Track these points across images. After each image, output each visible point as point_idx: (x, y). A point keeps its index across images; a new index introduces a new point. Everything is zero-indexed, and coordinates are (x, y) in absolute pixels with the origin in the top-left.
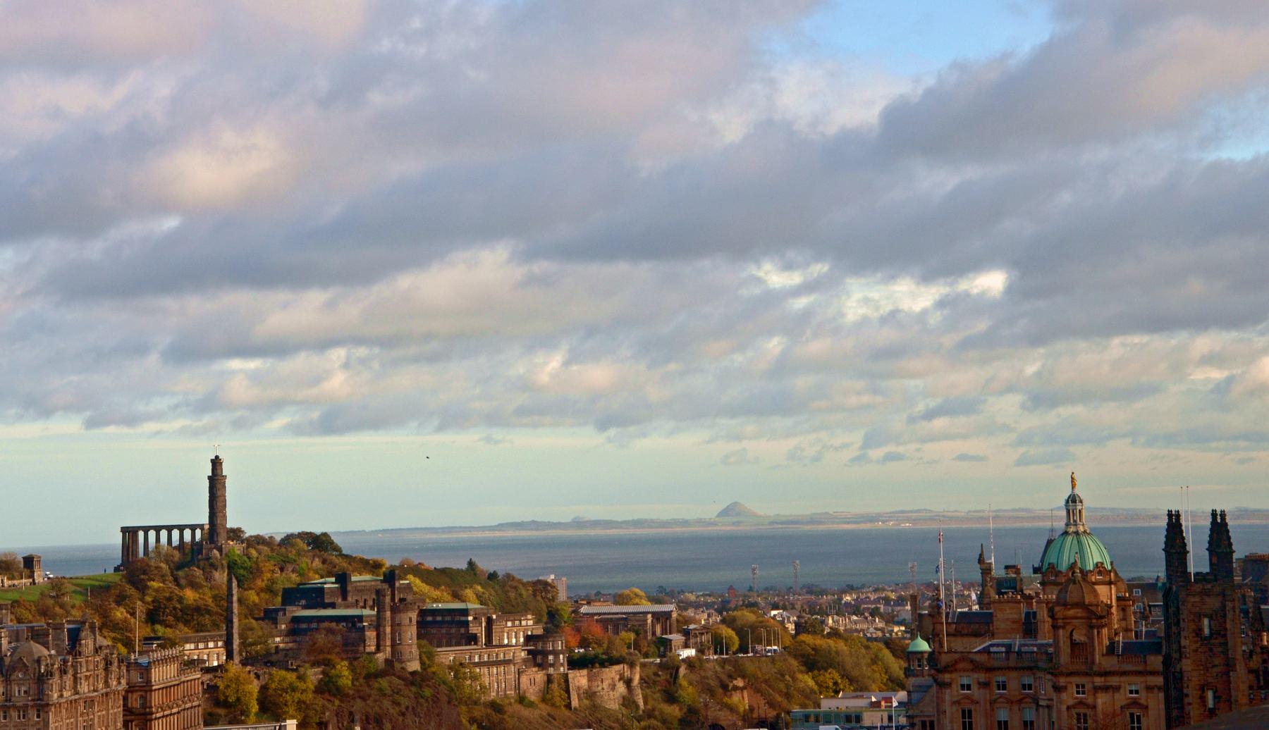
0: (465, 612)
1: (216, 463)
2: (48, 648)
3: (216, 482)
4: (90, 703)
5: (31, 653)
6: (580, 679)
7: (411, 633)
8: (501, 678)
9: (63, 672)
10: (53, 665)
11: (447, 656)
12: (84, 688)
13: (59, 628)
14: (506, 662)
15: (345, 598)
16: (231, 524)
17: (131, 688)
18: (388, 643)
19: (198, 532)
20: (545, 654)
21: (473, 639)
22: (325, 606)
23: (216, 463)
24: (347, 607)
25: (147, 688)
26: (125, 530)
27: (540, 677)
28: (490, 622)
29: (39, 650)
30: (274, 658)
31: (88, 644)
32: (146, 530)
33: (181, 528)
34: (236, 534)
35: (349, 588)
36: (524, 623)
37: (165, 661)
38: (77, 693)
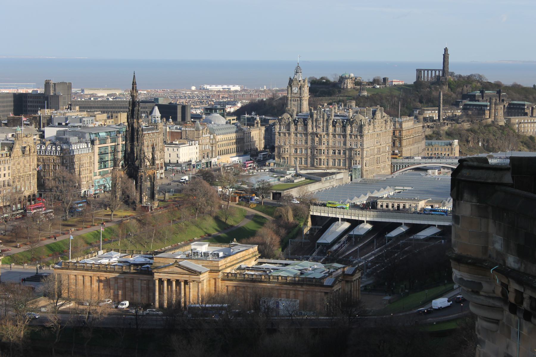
0: (524, 105)
1: (446, 50)
3: (446, 56)
7: (501, 113)
11: (515, 120)
12: (378, 130)
15: (483, 99)
18: (493, 115)
22: (476, 101)
23: (446, 50)
24: (483, 101)
26: (417, 70)
28: (533, 108)
30: (455, 118)
31: (378, 115)
32: (424, 70)
33: (435, 70)
34: (452, 74)
37: (408, 121)
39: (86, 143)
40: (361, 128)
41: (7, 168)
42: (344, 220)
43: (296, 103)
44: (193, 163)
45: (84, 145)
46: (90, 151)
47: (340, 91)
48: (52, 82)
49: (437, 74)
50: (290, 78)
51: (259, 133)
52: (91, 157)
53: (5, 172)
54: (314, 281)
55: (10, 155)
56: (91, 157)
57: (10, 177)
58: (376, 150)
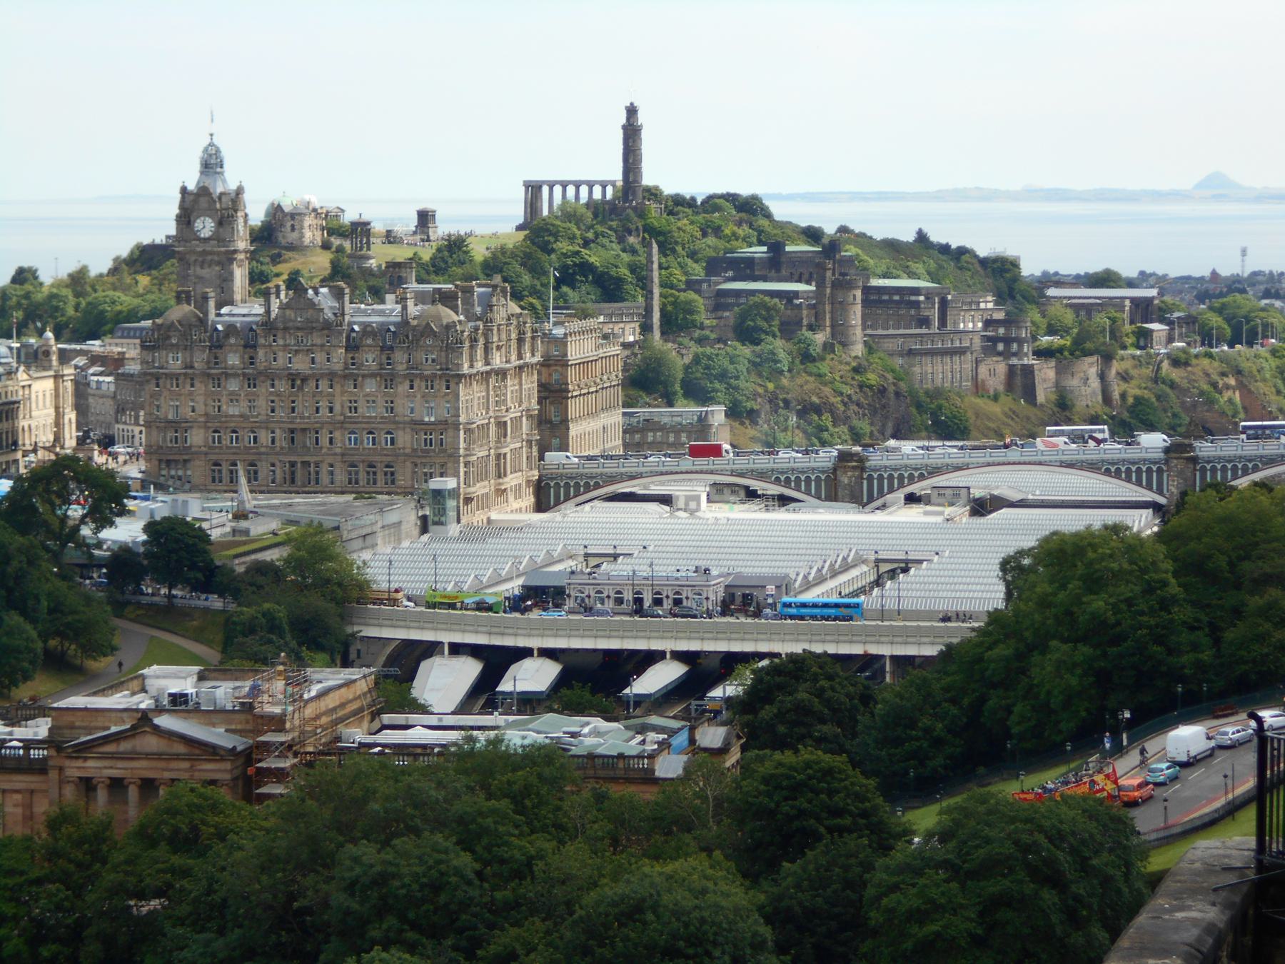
0: (916, 291)
1: (632, 111)
2: (457, 313)
3: (631, 133)
4: (502, 374)
5: (438, 318)
6: (1046, 373)
8: (957, 367)
10: (463, 332)
13: (469, 291)
14: (961, 352)
15: (778, 271)
16: (648, 179)
17: (547, 363)
19: (609, 190)
20: (1007, 341)
21: (925, 322)
22: (755, 279)
23: (632, 111)
24: (780, 280)
26: (528, 185)
27: (1001, 368)
28: (944, 303)
29: (448, 315)
32: (551, 185)
33: (591, 185)
34: (653, 193)
35: (783, 259)
36: (982, 306)
38: (487, 363)
42: (456, 649)
43: (205, 272)
47: (279, 255)
51: (56, 389)
54: (621, 765)
58: (493, 428)
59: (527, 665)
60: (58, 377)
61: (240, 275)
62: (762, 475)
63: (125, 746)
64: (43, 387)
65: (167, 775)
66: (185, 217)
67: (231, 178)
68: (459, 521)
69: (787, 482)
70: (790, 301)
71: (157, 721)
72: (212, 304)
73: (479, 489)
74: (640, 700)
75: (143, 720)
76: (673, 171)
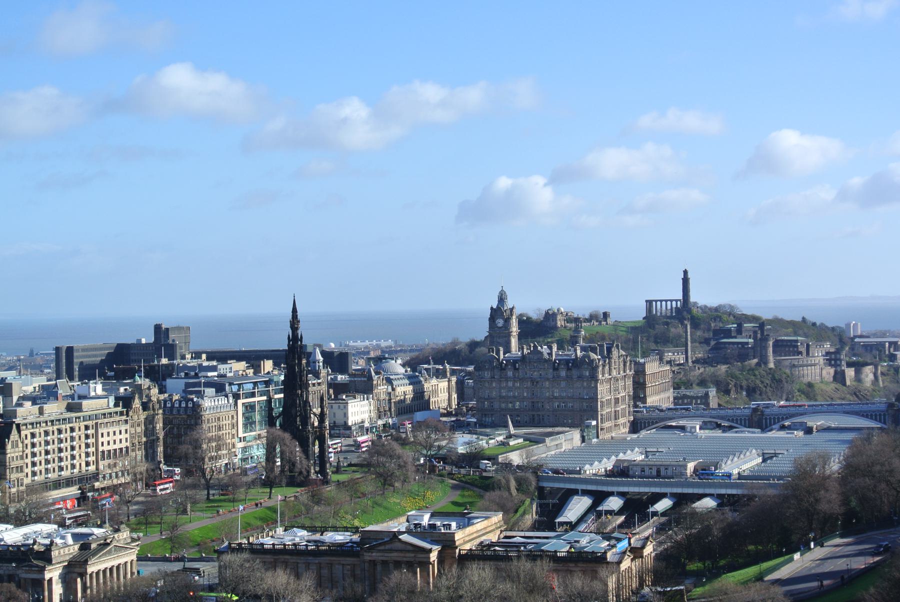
0: (797, 341)
1: (685, 272)
3: (686, 281)
9: (604, 366)
11: (788, 359)
12: (614, 373)
13: (601, 346)
14: (815, 365)
20: (836, 360)
21: (800, 353)
22: (732, 337)
23: (685, 272)
25: (643, 372)
26: (647, 301)
28: (808, 346)
29: (593, 356)
31: (615, 353)
32: (656, 301)
33: (671, 301)
39: (227, 396)
40: (594, 369)
41: (123, 432)
44: (367, 425)
45: (223, 401)
46: (232, 408)
48: (164, 326)
49: (674, 306)
50: (492, 308)
52: (233, 417)
53: (121, 437)
55: (127, 415)
56: (233, 417)
57: (128, 444)
58: (613, 401)
59: (611, 498)
60: (449, 381)
61: (514, 342)
62: (722, 418)
63: (388, 547)
64: (443, 384)
65: (405, 559)
66: (492, 319)
67: (509, 304)
68: (598, 437)
69: (733, 421)
70: (743, 346)
71: (400, 537)
72: (502, 353)
73: (607, 425)
74: (655, 514)
75: (395, 536)
76: (704, 296)
